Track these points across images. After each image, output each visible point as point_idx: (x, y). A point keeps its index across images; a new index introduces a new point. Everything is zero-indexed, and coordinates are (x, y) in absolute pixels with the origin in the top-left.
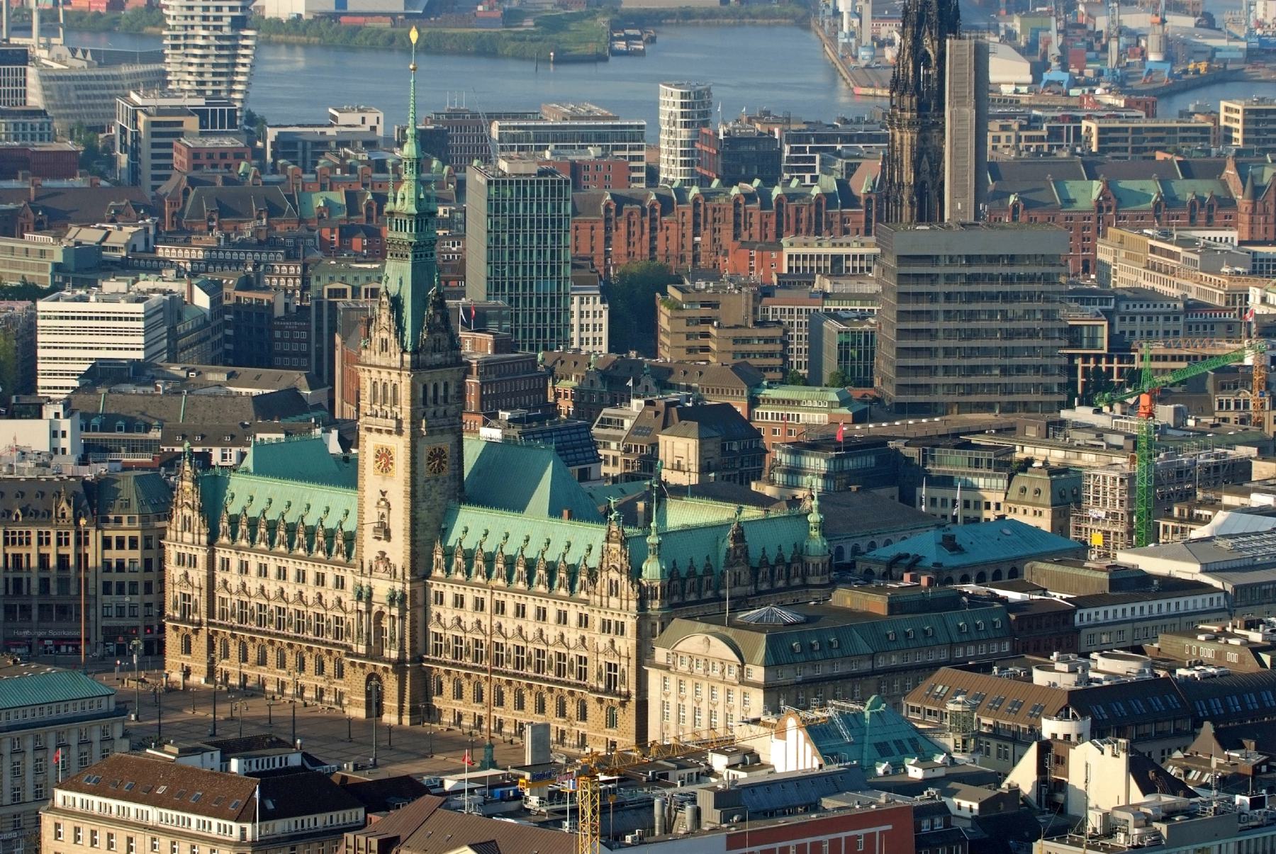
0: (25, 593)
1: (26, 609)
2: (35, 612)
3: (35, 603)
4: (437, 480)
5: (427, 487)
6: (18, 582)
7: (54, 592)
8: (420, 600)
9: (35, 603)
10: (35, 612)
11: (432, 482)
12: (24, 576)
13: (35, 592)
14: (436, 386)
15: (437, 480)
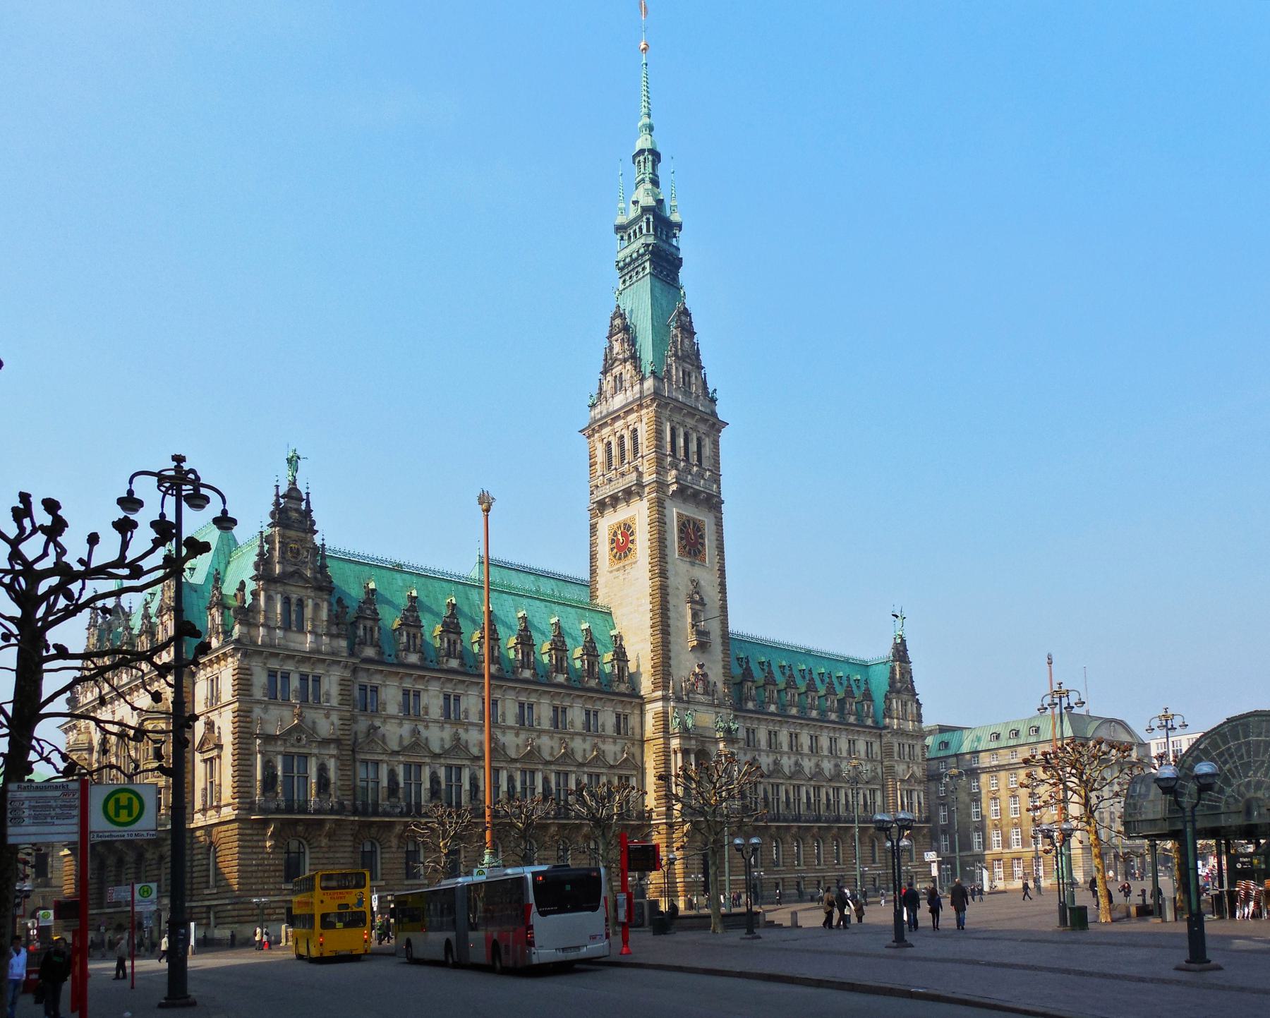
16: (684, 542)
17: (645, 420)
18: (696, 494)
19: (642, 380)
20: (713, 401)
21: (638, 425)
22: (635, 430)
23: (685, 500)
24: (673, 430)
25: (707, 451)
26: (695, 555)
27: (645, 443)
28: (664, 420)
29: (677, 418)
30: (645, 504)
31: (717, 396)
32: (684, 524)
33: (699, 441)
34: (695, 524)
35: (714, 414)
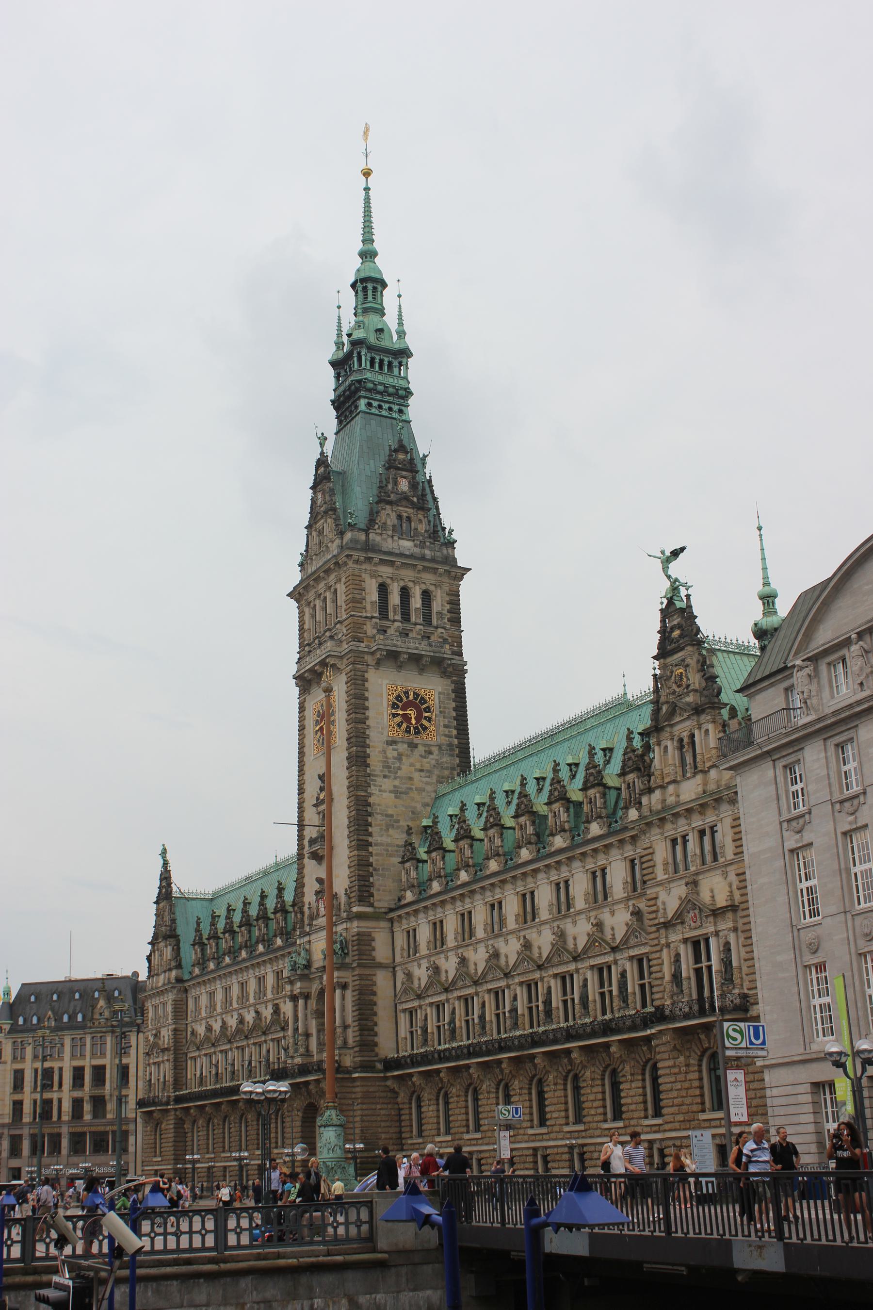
0: (55, 1118)
1: (55, 1141)
2: (65, 1143)
3: (65, 1130)
4: (413, 746)
5: (391, 753)
6: (48, 1103)
7: (87, 1117)
8: (381, 952)
9: (65, 1130)
10: (65, 1143)
11: (403, 748)
12: (55, 1096)
13: (65, 1118)
14: (405, 593)
15: (413, 746)
16: (398, 719)
17: (343, 580)
18: (415, 659)
19: (342, 534)
20: (451, 544)
21: (338, 586)
22: (336, 590)
23: (400, 667)
24: (383, 589)
25: (439, 604)
26: (417, 732)
27: (344, 607)
28: (366, 577)
29: (386, 571)
30: (343, 678)
31: (454, 536)
32: (398, 697)
33: (427, 596)
34: (416, 695)
35: (451, 561)
